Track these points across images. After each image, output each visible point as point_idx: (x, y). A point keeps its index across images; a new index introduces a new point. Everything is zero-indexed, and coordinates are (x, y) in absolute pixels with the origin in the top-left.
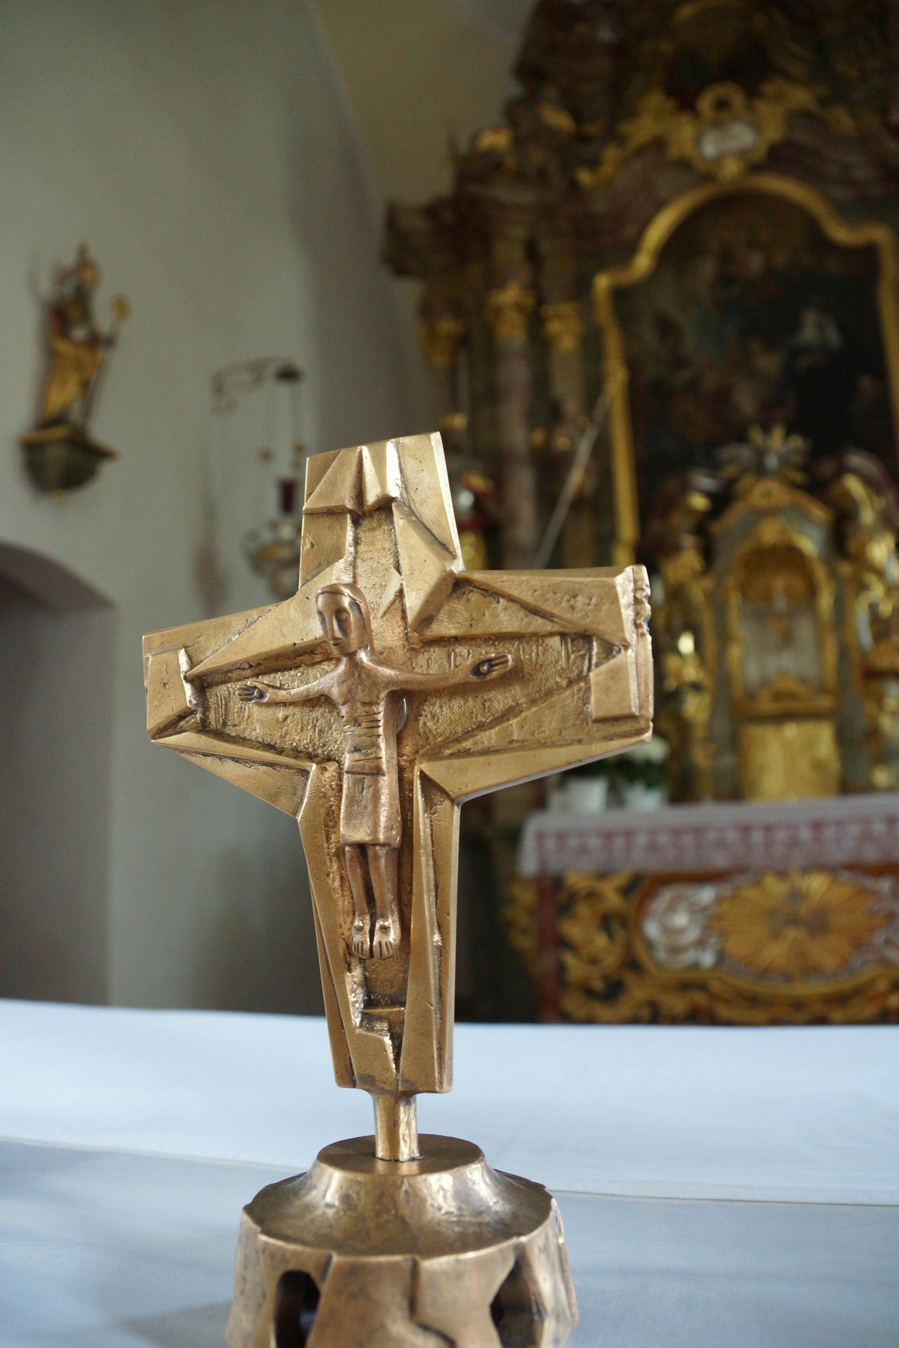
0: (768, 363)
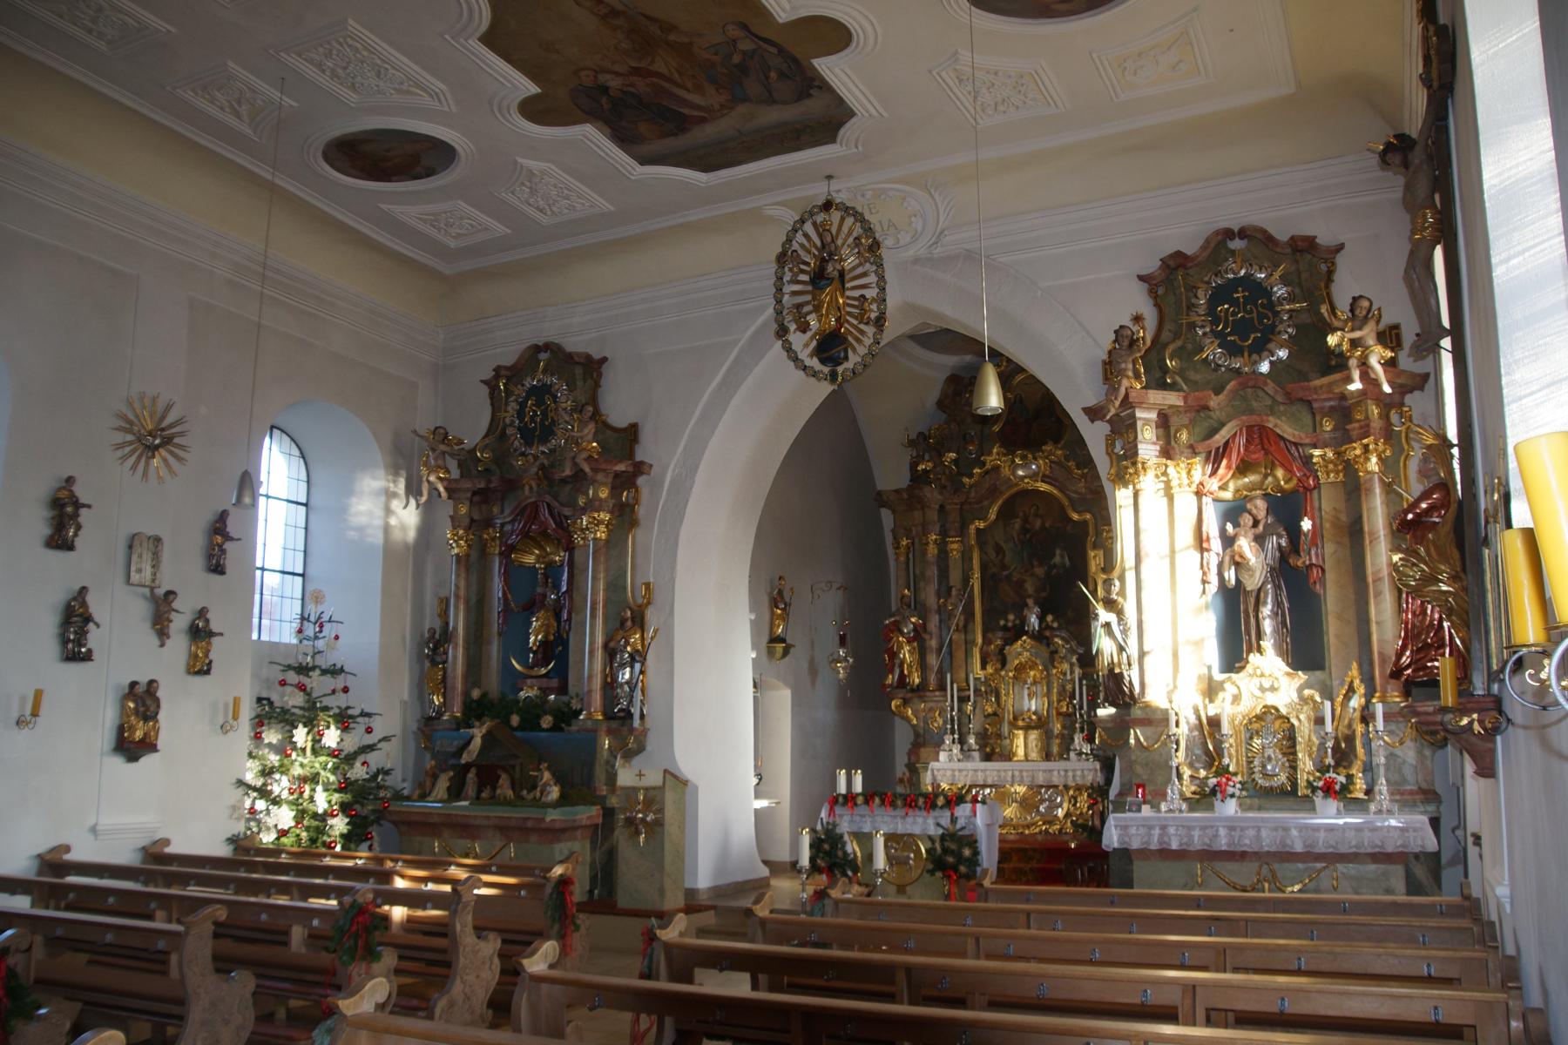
0: (1040, 571)
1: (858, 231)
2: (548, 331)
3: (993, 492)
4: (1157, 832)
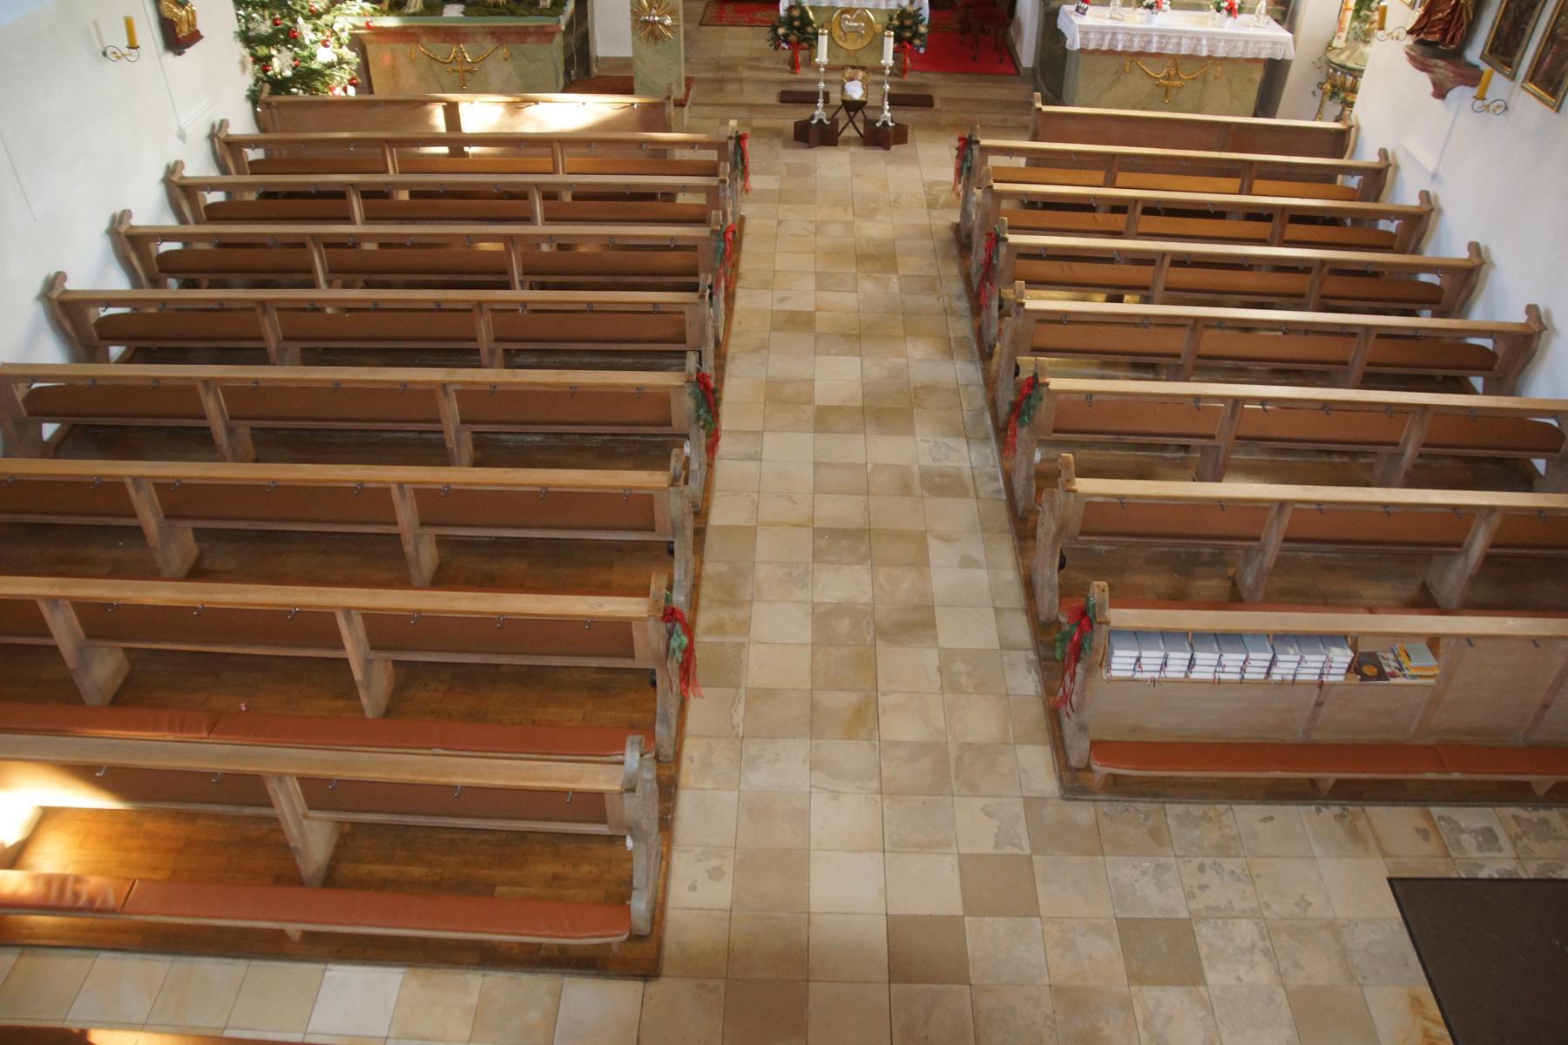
4: (1108, 37)
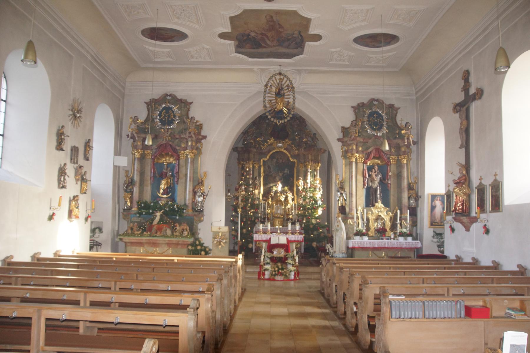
0: (281, 174)
1: (288, 82)
2: (170, 90)
3: (270, 151)
